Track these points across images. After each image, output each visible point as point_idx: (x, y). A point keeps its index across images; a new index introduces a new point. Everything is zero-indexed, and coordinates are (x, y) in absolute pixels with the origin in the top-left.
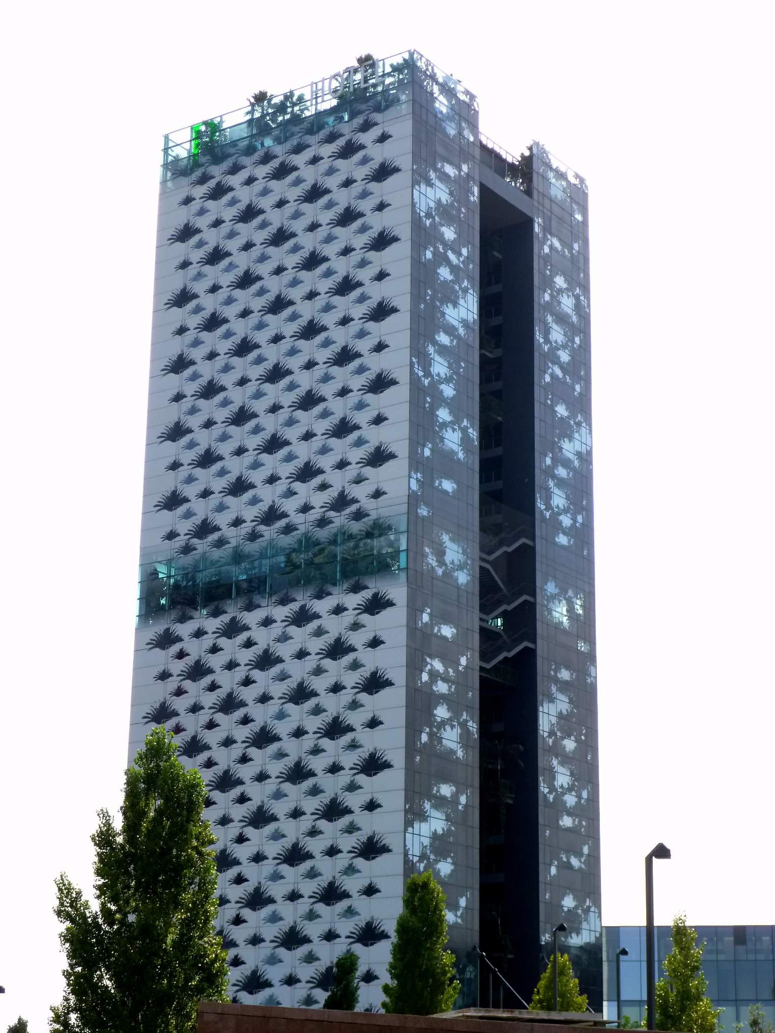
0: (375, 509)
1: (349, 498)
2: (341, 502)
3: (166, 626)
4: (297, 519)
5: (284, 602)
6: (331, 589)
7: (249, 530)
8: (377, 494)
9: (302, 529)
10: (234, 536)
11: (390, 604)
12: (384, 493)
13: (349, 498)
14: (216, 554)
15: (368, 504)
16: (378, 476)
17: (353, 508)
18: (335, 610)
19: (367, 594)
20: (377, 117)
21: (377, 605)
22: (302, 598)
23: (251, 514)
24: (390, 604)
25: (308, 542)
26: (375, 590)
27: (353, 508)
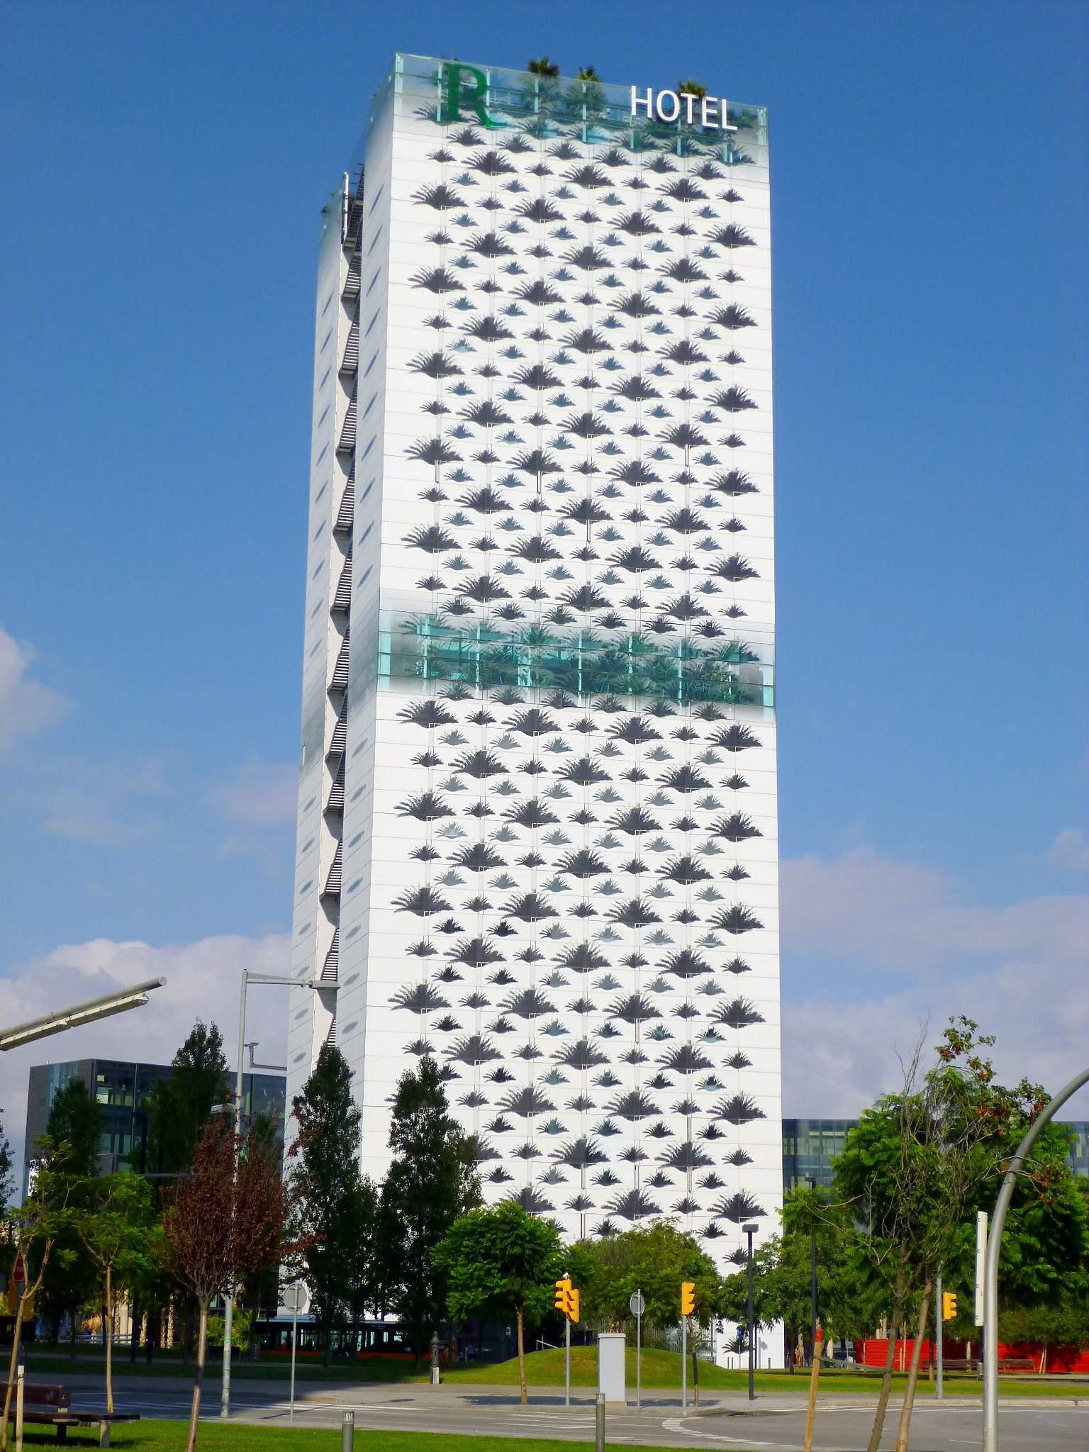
0: (732, 631)
1: (696, 606)
2: (685, 609)
3: (428, 699)
4: (625, 613)
5: (610, 707)
6: (673, 707)
7: (554, 608)
8: (734, 613)
9: (631, 627)
10: (534, 612)
11: (753, 743)
12: (742, 614)
13: (696, 606)
14: (503, 625)
15: (723, 622)
16: (732, 591)
17: (702, 620)
18: (683, 735)
19: (724, 725)
20: (718, 166)
21: (736, 740)
22: (633, 709)
23: (556, 589)
24: (753, 743)
25: (638, 644)
26: (733, 723)
27: (702, 620)
